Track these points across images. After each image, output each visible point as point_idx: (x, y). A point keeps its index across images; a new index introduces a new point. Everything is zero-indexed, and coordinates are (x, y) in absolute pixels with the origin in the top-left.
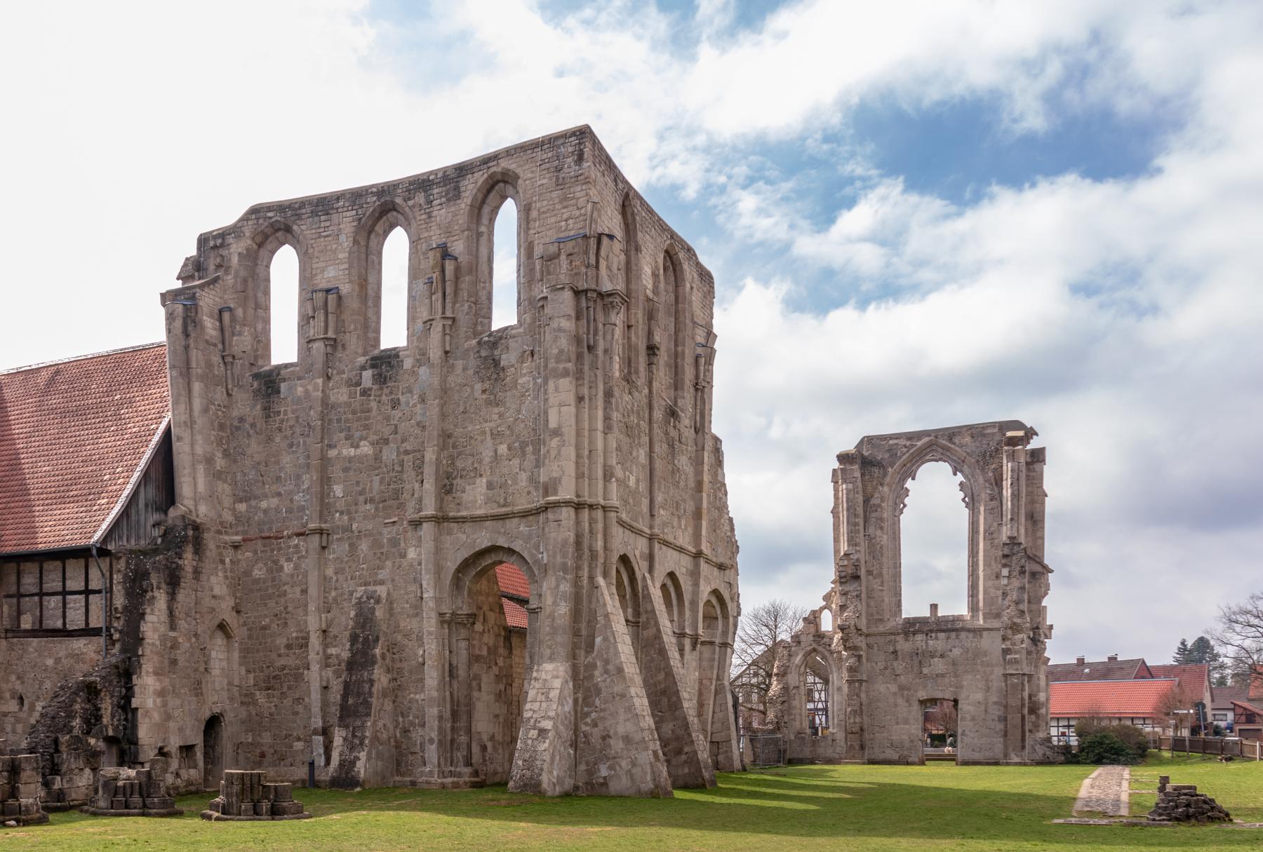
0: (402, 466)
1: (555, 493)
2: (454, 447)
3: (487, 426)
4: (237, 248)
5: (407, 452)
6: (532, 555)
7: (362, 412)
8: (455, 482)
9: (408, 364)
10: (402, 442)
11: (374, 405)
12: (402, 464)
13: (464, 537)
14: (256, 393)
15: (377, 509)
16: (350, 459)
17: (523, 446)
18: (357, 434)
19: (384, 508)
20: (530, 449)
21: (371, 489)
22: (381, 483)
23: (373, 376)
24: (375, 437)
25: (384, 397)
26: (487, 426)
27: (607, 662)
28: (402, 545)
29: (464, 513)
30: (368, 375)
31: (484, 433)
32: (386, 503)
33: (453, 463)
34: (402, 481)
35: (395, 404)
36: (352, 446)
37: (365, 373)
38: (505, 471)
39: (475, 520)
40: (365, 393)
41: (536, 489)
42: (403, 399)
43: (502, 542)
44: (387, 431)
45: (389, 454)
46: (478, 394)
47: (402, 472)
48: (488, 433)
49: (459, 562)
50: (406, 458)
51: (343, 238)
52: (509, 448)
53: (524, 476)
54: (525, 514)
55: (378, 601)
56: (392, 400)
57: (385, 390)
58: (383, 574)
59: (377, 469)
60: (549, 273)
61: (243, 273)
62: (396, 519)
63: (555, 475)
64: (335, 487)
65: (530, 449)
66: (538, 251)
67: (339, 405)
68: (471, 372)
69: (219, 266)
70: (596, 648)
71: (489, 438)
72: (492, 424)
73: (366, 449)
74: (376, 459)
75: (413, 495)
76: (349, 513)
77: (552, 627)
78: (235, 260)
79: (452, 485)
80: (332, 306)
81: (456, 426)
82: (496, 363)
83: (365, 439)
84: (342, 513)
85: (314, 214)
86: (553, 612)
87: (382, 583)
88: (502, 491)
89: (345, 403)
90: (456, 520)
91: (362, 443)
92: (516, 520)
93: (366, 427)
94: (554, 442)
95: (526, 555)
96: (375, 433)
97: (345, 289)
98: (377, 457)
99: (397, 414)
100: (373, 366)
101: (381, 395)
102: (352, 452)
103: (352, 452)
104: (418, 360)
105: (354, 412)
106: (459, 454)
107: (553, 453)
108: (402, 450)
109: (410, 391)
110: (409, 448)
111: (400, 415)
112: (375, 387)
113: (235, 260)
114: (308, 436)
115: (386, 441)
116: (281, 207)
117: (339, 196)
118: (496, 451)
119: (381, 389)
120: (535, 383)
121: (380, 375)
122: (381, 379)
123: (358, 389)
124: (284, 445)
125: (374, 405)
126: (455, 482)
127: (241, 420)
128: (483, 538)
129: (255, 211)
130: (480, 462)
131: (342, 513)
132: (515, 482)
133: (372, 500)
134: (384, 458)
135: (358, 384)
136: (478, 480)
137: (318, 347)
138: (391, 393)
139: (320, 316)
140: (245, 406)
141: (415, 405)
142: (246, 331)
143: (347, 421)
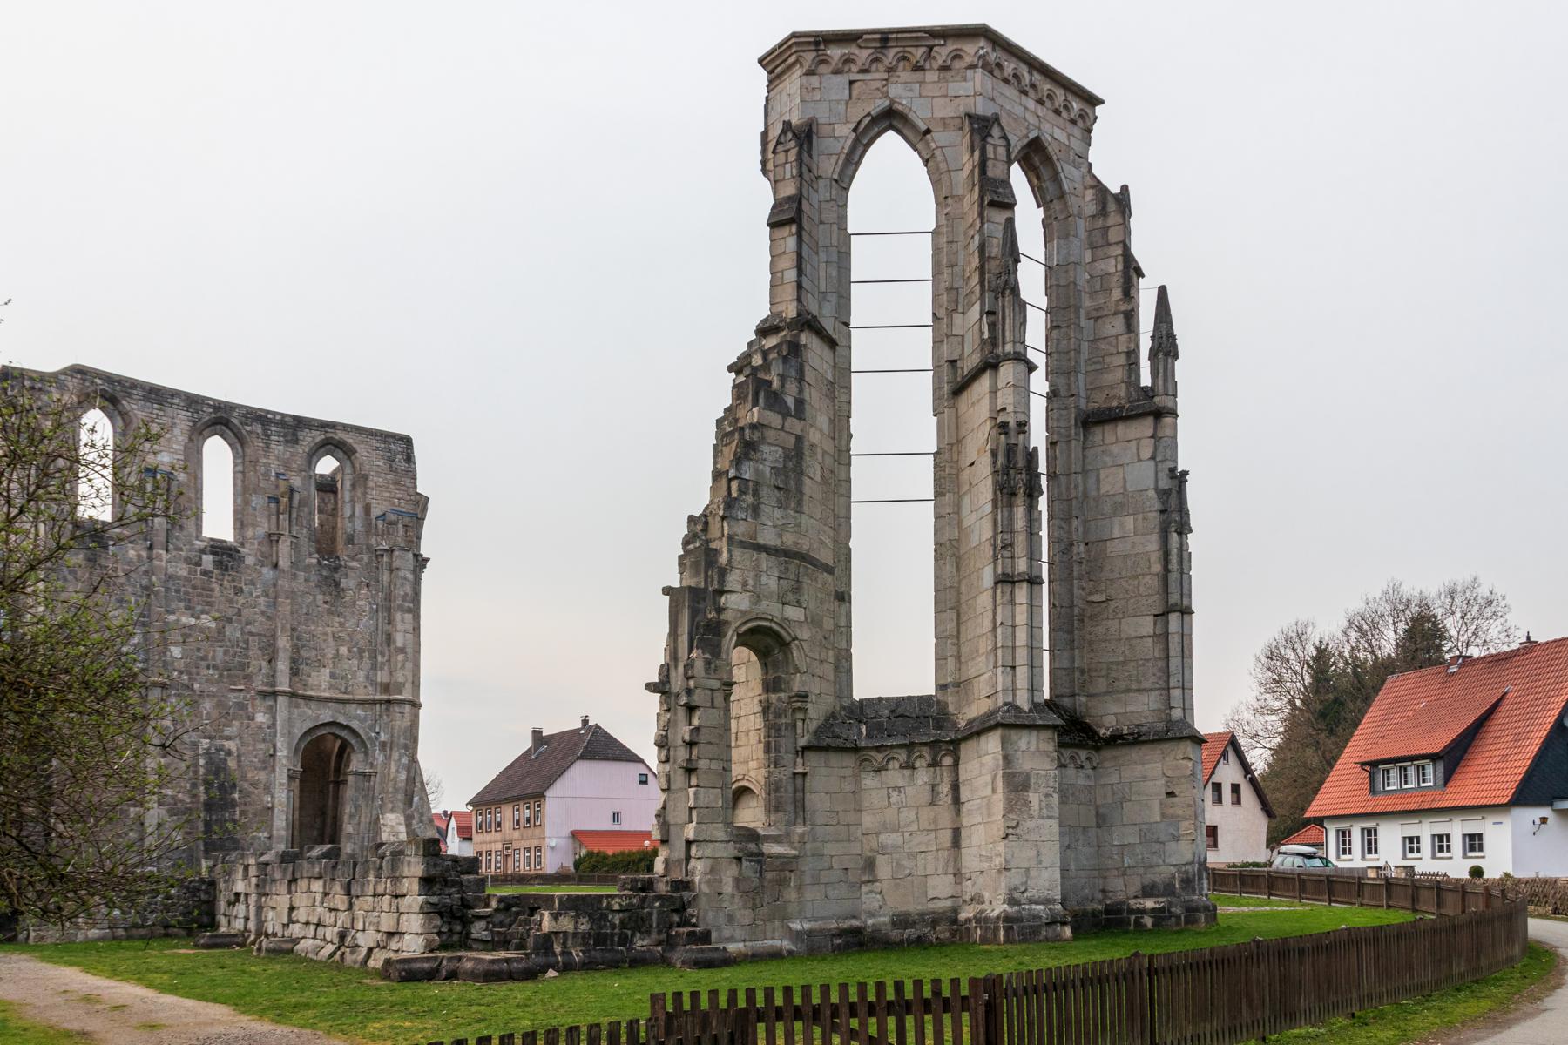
0: (247, 644)
1: (400, 693)
2: (298, 639)
3: (329, 630)
5: (251, 634)
6: (367, 734)
7: (203, 589)
8: (301, 667)
9: (250, 561)
10: (247, 625)
11: (216, 587)
12: (247, 642)
13: (310, 712)
15: (221, 675)
16: (191, 627)
17: (361, 651)
18: (199, 608)
19: (229, 676)
20: (366, 654)
21: (214, 658)
22: (226, 653)
23: (214, 561)
24: (217, 615)
25: (225, 582)
26: (329, 630)
27: (422, 815)
28: (250, 709)
29: (312, 693)
30: (208, 560)
31: (326, 634)
32: (232, 672)
33: (298, 652)
34: (248, 657)
35: (239, 591)
36: (192, 616)
37: (204, 557)
38: (346, 667)
39: (320, 700)
40: (205, 573)
41: (371, 685)
42: (246, 589)
43: (342, 720)
44: (230, 612)
45: (233, 632)
46: (320, 602)
47: (247, 648)
48: (330, 635)
49: (304, 730)
50: (251, 638)
52: (349, 650)
53: (361, 675)
54: (362, 702)
55: (229, 753)
56: (235, 587)
57: (227, 577)
58: (229, 731)
59: (219, 641)
60: (389, 533)
62: (242, 687)
63: (400, 680)
64: (172, 648)
65: (366, 654)
66: (375, 512)
67: (179, 578)
68: (313, 584)
70: (414, 805)
71: (331, 639)
72: (334, 629)
73: (206, 621)
74: (219, 633)
75: (260, 670)
76: (189, 673)
77: (395, 788)
79: (298, 669)
81: (300, 623)
82: (337, 584)
83: (207, 613)
84: (181, 672)
86: (396, 777)
87: (229, 738)
88: (343, 682)
89: (185, 577)
90: (303, 697)
91: (203, 616)
92: (354, 705)
93: (208, 604)
94: (401, 657)
95: (361, 732)
96: (217, 611)
98: (221, 631)
99: (241, 600)
100: (213, 553)
101: (222, 580)
102: (193, 621)
103: (193, 621)
104: (260, 561)
105: (194, 587)
106: (303, 646)
107: (399, 665)
108: (246, 631)
109: (253, 583)
110: (253, 630)
111: (243, 601)
112: (215, 571)
114: (141, 596)
115: (230, 620)
118: (337, 650)
119: (224, 575)
120: (372, 608)
121: (221, 562)
122: (219, 564)
123: (199, 569)
125: (216, 587)
126: (301, 667)
128: (326, 715)
130: (323, 656)
131: (181, 672)
132: (354, 677)
133: (214, 667)
134: (228, 633)
135: (199, 564)
136: (322, 670)
138: (233, 581)
141: (258, 597)
143: (187, 593)
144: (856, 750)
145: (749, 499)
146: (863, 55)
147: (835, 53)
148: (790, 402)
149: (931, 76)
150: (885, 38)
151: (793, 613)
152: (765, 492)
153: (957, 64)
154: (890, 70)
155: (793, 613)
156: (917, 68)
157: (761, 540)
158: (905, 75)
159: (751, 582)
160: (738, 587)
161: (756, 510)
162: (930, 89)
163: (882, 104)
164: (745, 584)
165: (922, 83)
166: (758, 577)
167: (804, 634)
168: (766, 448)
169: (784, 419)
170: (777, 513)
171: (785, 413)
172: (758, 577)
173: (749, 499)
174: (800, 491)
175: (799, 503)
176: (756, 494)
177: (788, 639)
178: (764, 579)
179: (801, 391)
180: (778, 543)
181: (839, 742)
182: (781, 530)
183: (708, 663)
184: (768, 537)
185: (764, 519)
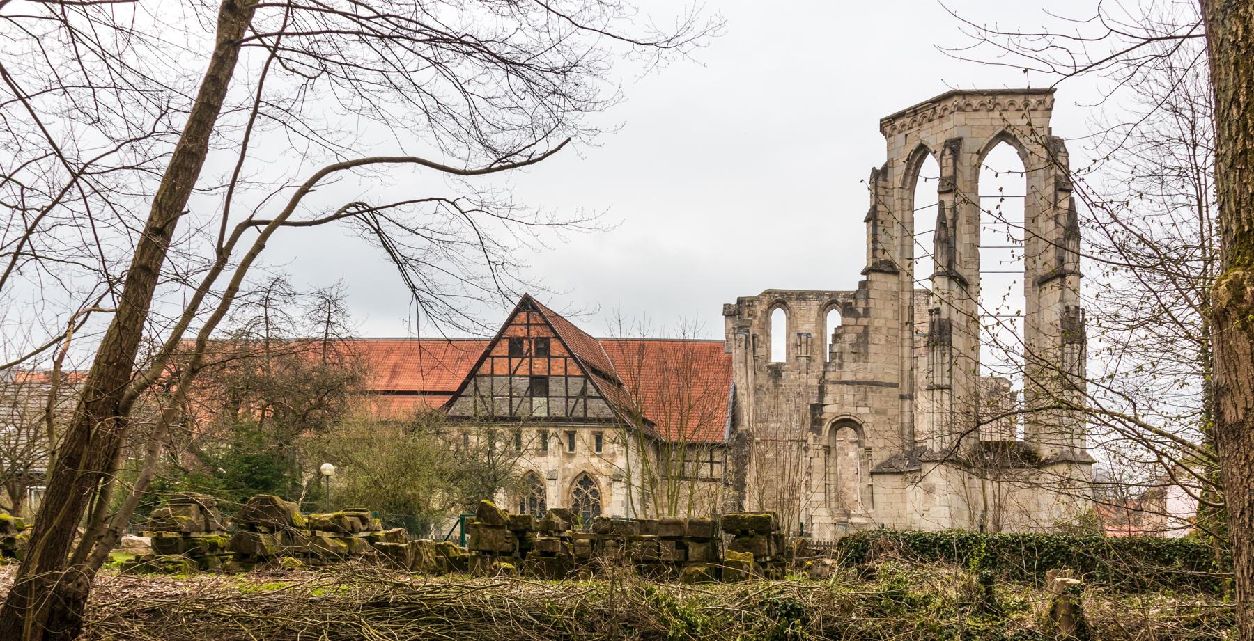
4: (760, 309)
14: (770, 375)
51: (812, 312)
61: (763, 320)
69: (750, 315)
78: (759, 314)
80: (809, 343)
85: (798, 299)
97: (814, 335)
113: (759, 314)
116: (782, 293)
117: (811, 293)
124: (784, 400)
127: (761, 386)
129: (769, 292)
137: (803, 360)
139: (804, 346)
140: (763, 379)
142: (764, 346)
144: (901, 473)
145: (837, 361)
146: (908, 120)
147: (898, 123)
148: (861, 311)
149: (936, 122)
150: (915, 111)
151: (862, 410)
152: (845, 356)
153: (947, 113)
154: (920, 125)
155: (862, 410)
156: (930, 120)
157: (843, 379)
158: (926, 125)
159: (838, 399)
160: (831, 402)
161: (841, 366)
162: (936, 130)
163: (917, 143)
164: (835, 400)
165: (932, 127)
166: (842, 396)
167: (869, 419)
168: (846, 336)
169: (857, 319)
170: (853, 365)
171: (857, 316)
172: (842, 396)
173: (837, 361)
174: (867, 353)
175: (866, 358)
176: (841, 358)
177: (860, 422)
178: (845, 397)
179: (867, 303)
180: (854, 378)
181: (891, 470)
182: (855, 373)
183: (815, 438)
184: (848, 376)
185: (845, 369)
